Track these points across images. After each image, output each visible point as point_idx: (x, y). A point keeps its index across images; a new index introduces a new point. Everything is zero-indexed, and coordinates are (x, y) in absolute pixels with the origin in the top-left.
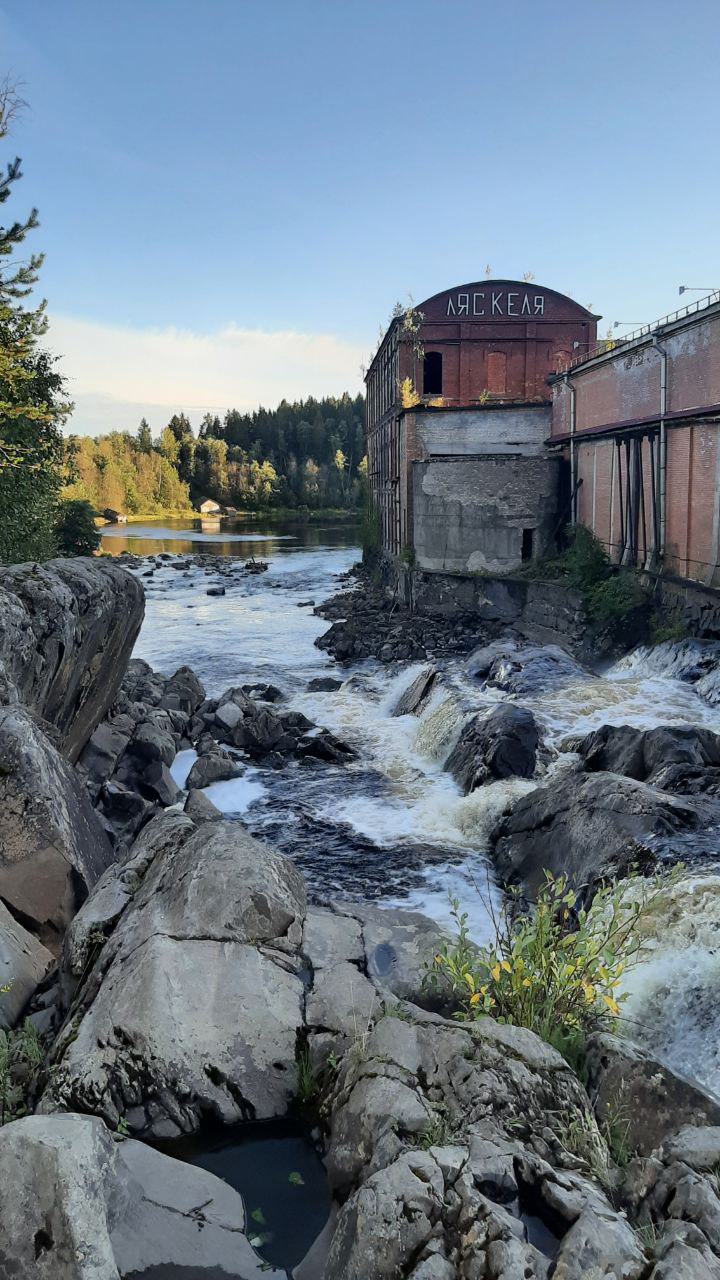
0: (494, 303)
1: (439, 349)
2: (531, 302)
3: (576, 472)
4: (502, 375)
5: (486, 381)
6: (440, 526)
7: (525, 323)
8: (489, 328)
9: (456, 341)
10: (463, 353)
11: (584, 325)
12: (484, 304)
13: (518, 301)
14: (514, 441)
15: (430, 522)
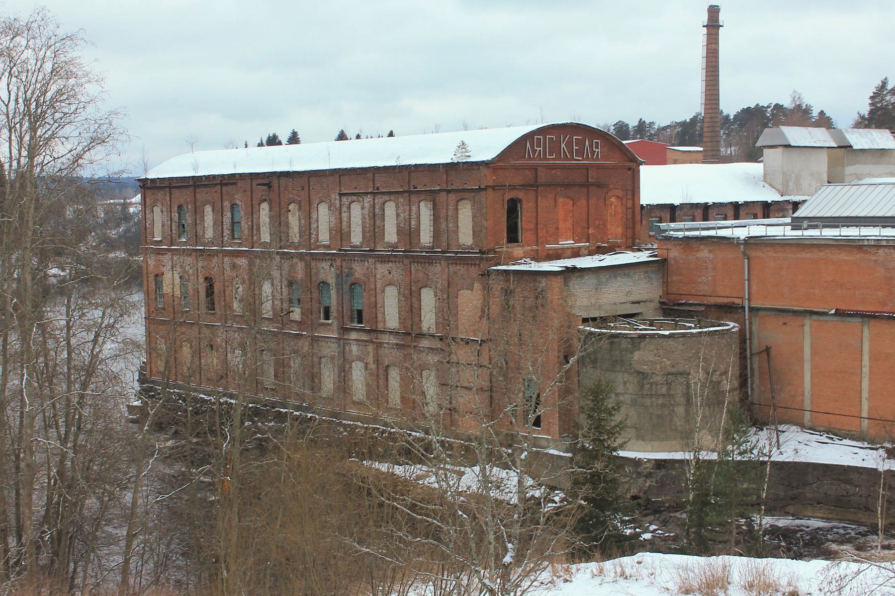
0: (563, 146)
1: (520, 195)
2: (591, 146)
3: (750, 339)
4: (569, 223)
5: (557, 228)
6: (663, 406)
7: (587, 168)
8: (559, 172)
9: (533, 186)
10: (539, 198)
11: (629, 169)
12: (555, 147)
13: (581, 143)
14: (637, 299)
15: (648, 402)
